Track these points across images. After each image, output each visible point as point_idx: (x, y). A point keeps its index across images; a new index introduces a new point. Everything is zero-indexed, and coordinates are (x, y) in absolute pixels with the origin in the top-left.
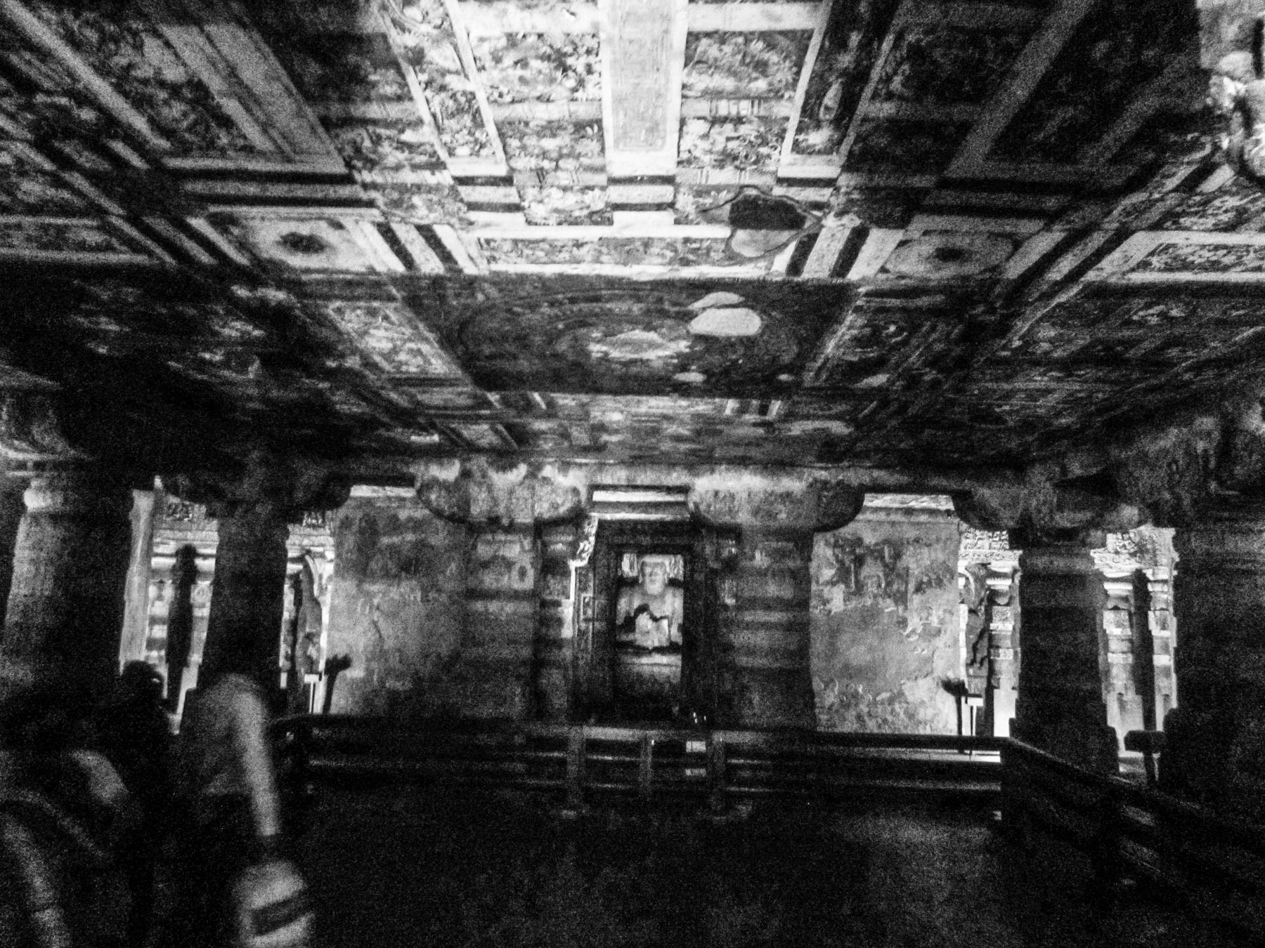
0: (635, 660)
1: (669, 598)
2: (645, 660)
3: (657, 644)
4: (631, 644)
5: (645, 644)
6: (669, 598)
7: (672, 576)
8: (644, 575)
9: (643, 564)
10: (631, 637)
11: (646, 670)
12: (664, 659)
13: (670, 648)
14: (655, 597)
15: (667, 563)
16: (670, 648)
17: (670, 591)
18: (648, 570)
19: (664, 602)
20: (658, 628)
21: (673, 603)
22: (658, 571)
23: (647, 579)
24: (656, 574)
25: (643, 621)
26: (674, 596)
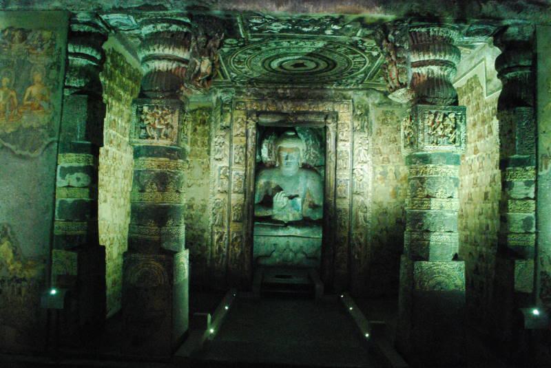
0: (274, 233)
1: (302, 180)
2: (281, 232)
3: (291, 219)
4: (269, 219)
5: (280, 219)
6: (302, 180)
7: (304, 161)
8: (280, 161)
9: (280, 149)
10: (269, 213)
11: (282, 242)
12: (298, 232)
13: (303, 222)
14: (290, 178)
15: (301, 149)
16: (303, 222)
17: (303, 173)
18: (284, 154)
19: (298, 182)
20: (293, 205)
21: (305, 184)
22: (293, 154)
23: (284, 162)
24: (292, 158)
25: (280, 200)
26: (307, 177)
